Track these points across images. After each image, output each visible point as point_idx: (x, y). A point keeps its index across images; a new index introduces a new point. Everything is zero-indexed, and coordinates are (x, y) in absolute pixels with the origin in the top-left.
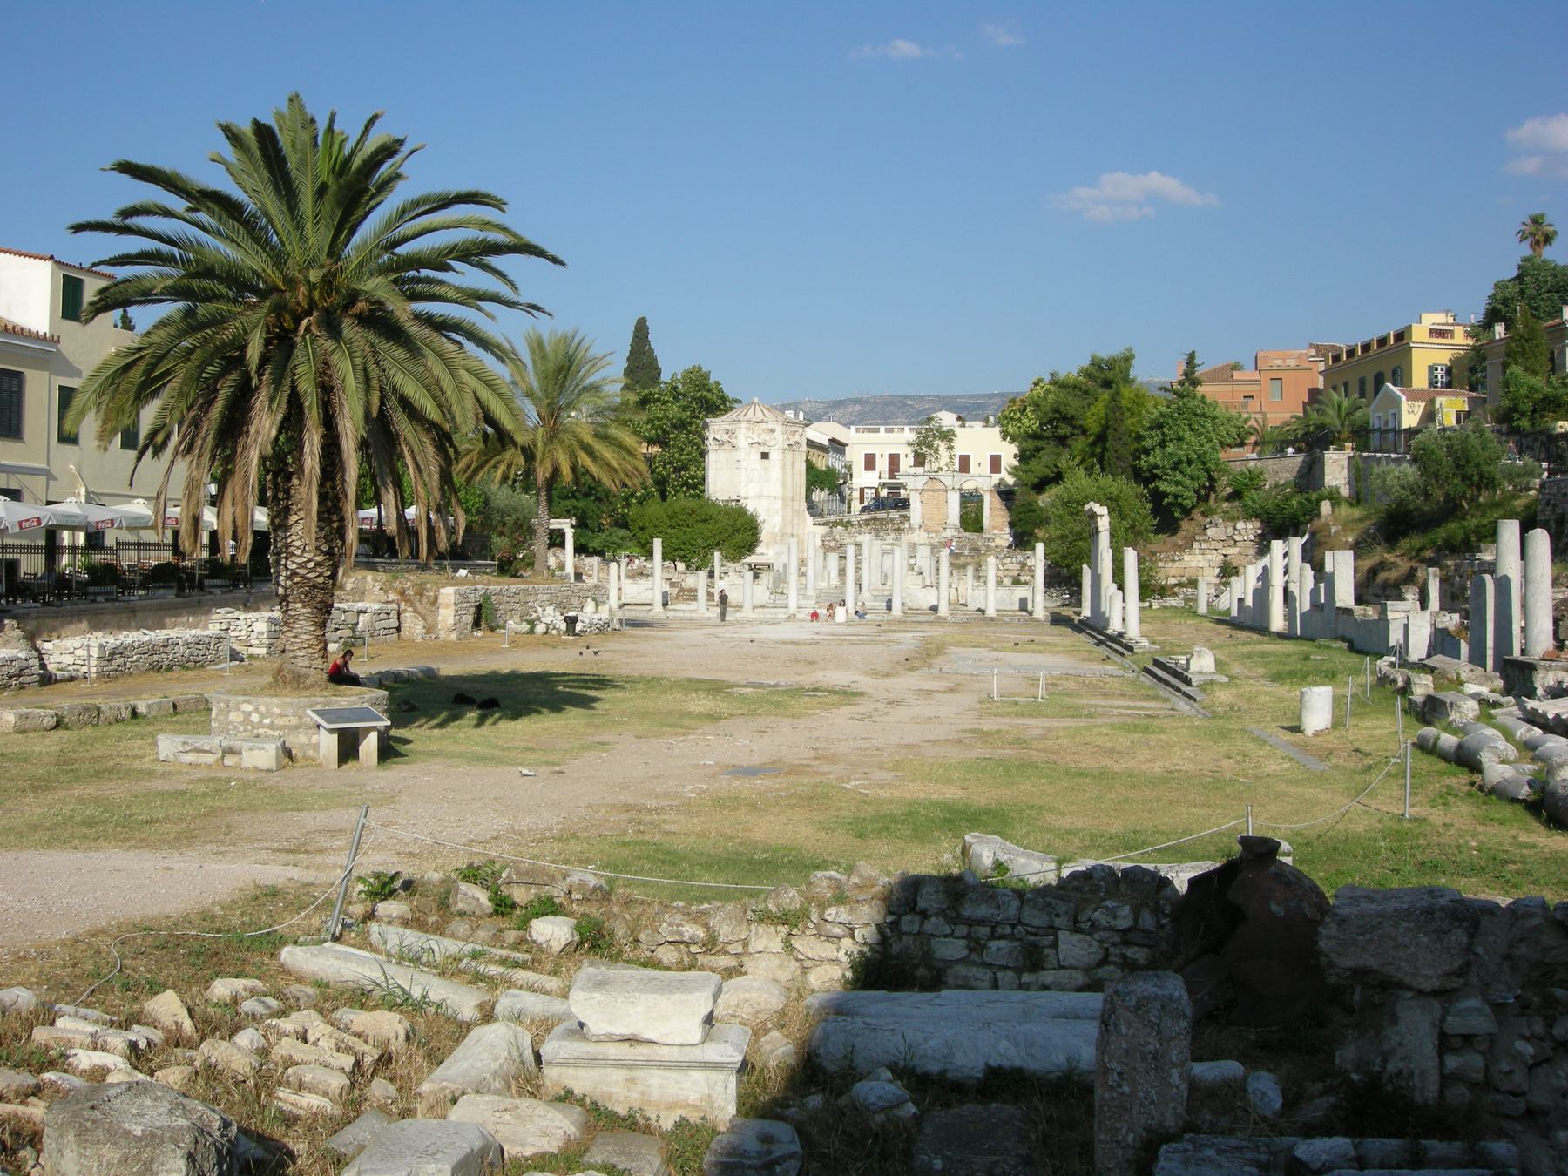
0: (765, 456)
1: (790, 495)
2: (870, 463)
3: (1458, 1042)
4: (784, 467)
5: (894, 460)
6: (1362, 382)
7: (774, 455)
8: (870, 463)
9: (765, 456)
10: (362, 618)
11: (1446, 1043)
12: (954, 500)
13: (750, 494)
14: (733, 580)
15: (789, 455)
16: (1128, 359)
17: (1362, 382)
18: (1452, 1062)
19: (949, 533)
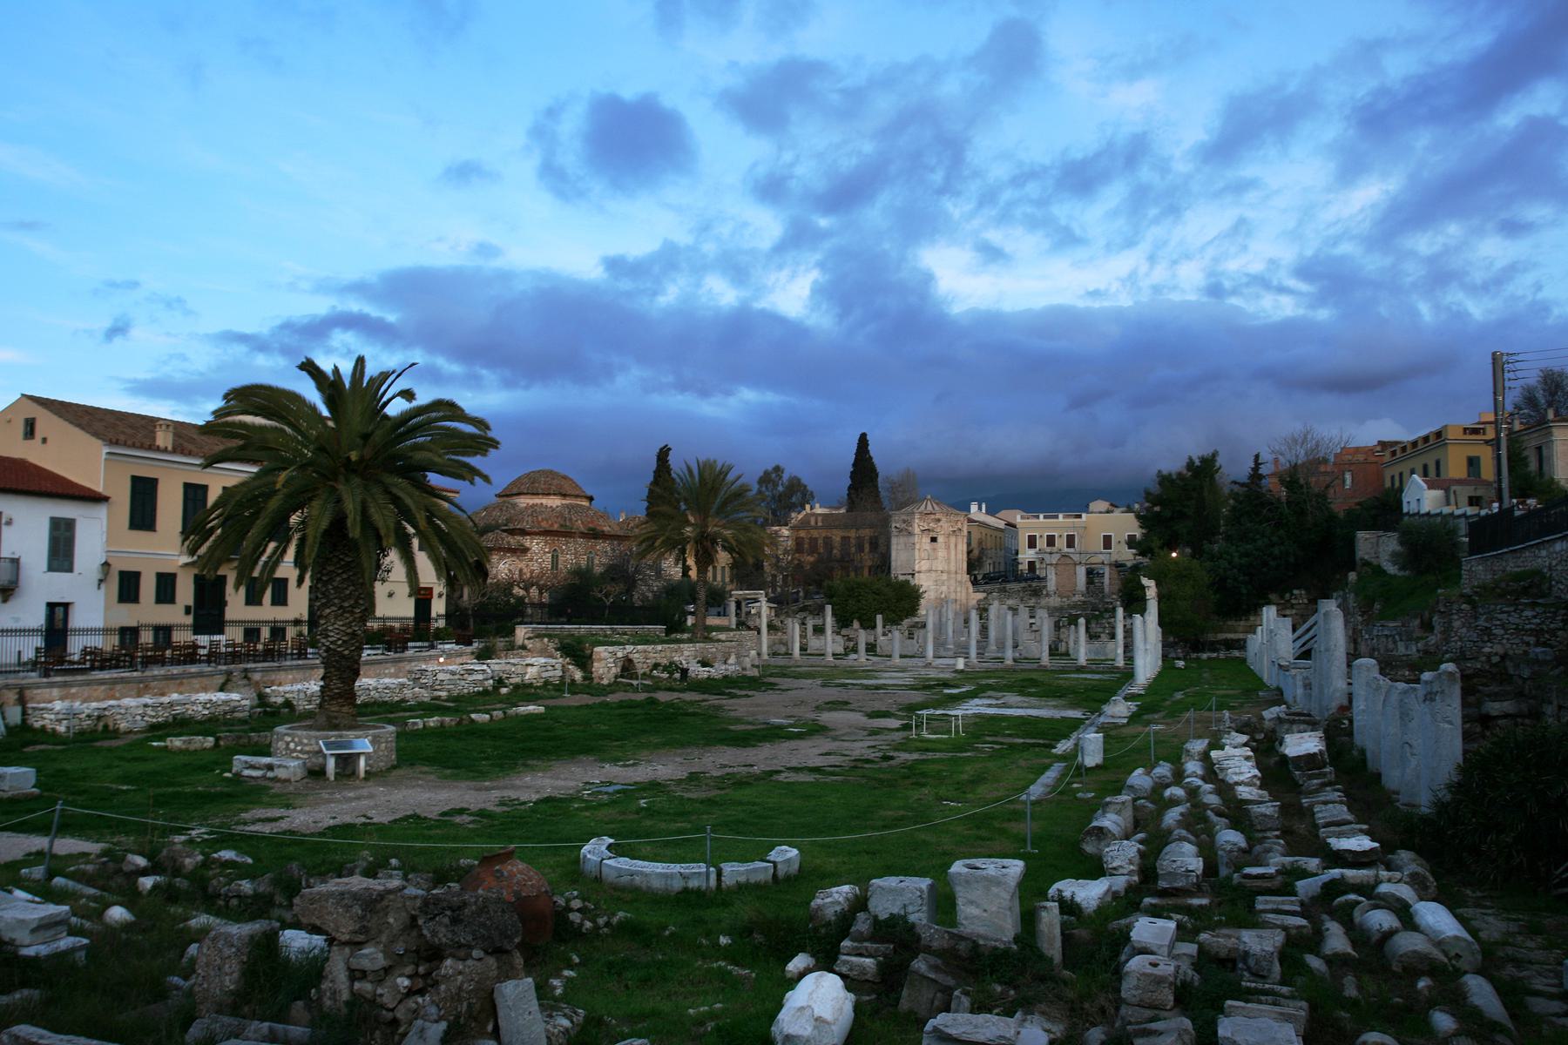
0: (934, 540)
1: (953, 569)
2: (1032, 542)
3: (358, 974)
4: (948, 548)
5: (1051, 541)
6: (1425, 467)
7: (940, 539)
8: (1032, 542)
9: (934, 540)
10: (530, 669)
11: (355, 974)
12: (1081, 572)
13: (924, 568)
14: (893, 640)
15: (953, 539)
16: (1215, 455)
17: (1425, 467)
18: (357, 985)
19: (1077, 598)
